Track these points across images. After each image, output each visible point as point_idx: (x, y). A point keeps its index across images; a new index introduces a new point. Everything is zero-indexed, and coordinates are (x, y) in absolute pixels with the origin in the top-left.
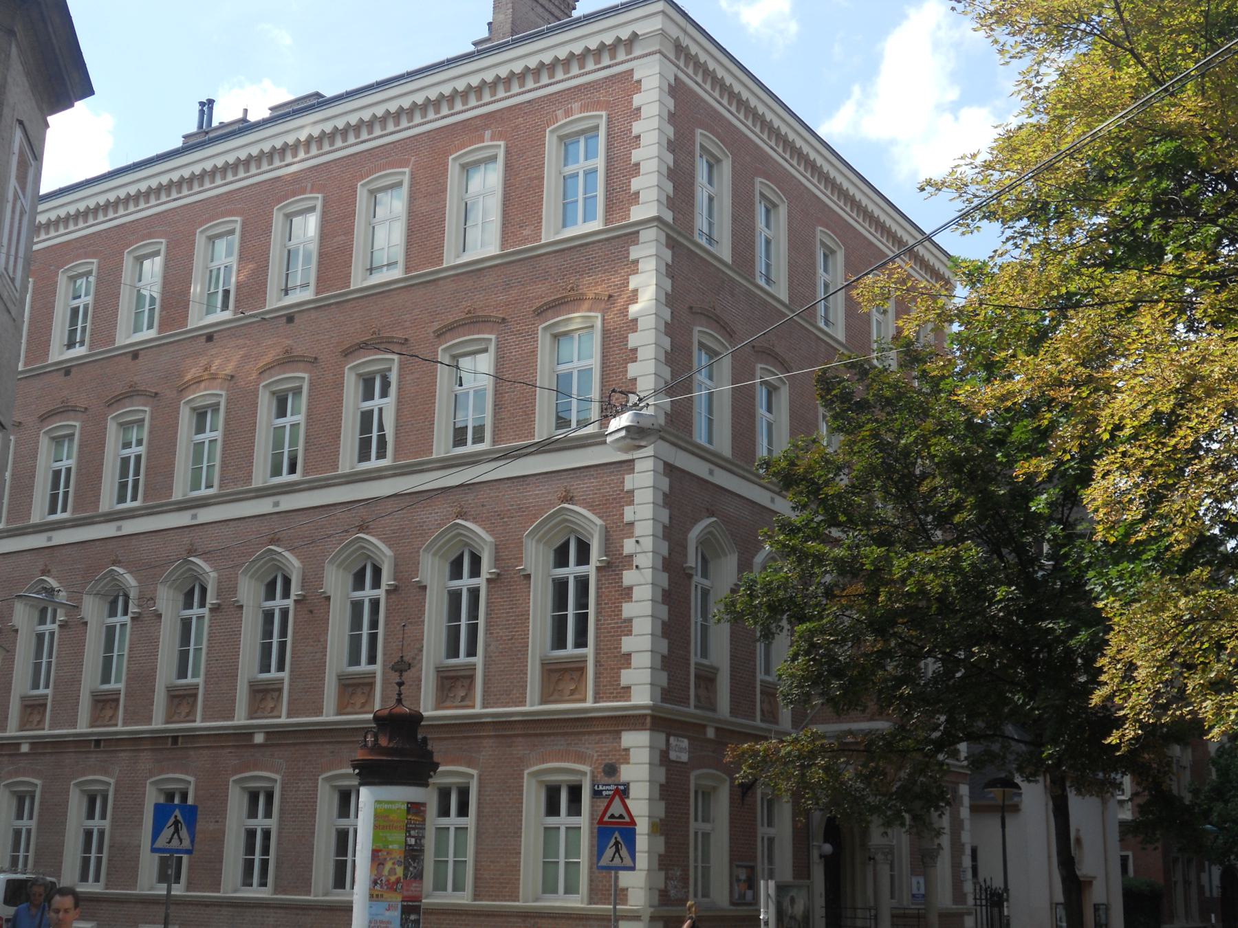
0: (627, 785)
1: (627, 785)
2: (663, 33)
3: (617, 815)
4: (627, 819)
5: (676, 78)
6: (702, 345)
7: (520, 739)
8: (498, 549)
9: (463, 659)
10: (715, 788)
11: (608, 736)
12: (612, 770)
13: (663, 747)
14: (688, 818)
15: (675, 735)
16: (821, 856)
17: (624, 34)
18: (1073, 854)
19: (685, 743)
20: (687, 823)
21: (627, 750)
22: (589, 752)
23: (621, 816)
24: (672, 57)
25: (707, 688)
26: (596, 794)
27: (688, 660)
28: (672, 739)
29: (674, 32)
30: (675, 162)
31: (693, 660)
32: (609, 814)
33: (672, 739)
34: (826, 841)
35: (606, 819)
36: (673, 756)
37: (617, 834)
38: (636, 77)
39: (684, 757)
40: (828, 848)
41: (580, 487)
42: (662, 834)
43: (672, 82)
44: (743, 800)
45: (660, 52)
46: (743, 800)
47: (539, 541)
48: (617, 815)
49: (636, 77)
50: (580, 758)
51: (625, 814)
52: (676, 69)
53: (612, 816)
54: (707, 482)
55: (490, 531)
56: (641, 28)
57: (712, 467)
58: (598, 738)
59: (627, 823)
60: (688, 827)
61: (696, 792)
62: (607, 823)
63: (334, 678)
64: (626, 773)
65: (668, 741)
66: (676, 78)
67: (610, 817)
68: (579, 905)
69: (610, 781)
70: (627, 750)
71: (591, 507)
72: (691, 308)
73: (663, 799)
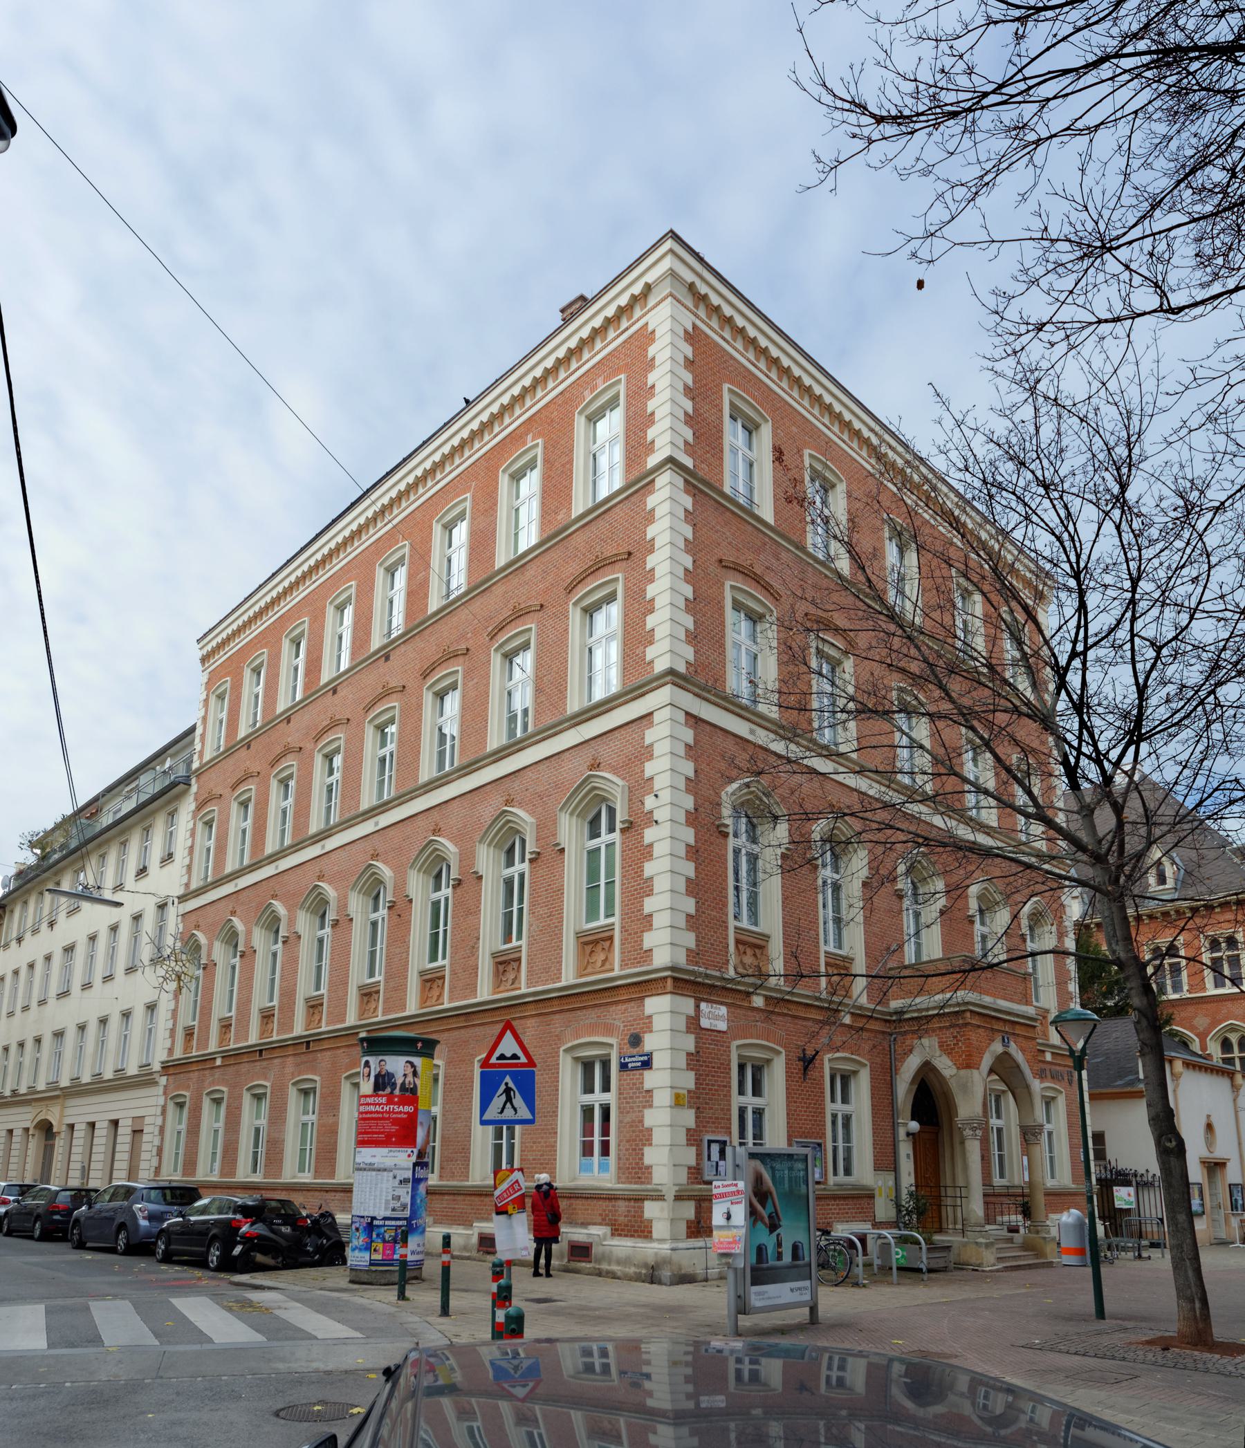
0: (650, 1055)
1: (650, 1055)
2: (672, 273)
3: (508, 1055)
4: (523, 1060)
5: (695, 327)
6: (737, 606)
7: (557, 1016)
8: (540, 827)
9: (514, 943)
10: (769, 1061)
11: (632, 1004)
12: (636, 1040)
13: (692, 1012)
14: (729, 1091)
15: (707, 1001)
16: (908, 1134)
17: (637, 289)
18: (1172, 1105)
19: (723, 1010)
20: (728, 1096)
21: (650, 1017)
22: (617, 1023)
23: (515, 1057)
24: (691, 305)
25: (755, 955)
26: (623, 1066)
27: (725, 922)
28: (703, 1005)
29: (689, 277)
30: (695, 409)
31: (732, 923)
32: (497, 1054)
33: (703, 1005)
34: (913, 1119)
35: (493, 1060)
36: (705, 1023)
37: (508, 1079)
38: (650, 328)
39: (722, 1026)
40: (914, 1126)
41: (605, 751)
42: (690, 1107)
43: (690, 330)
44: (805, 1074)
45: (671, 295)
46: (805, 1074)
47: (572, 814)
48: (508, 1055)
49: (650, 328)
50: (609, 1030)
51: (520, 1053)
52: (693, 318)
53: (502, 1057)
54: (748, 741)
55: (532, 813)
56: (650, 278)
57: (754, 727)
58: (624, 1007)
59: (523, 1065)
60: (729, 1101)
61: (742, 1067)
62: (494, 1065)
63: (415, 974)
64: (650, 1042)
65: (697, 1007)
66: (695, 327)
67: (498, 1059)
68: (609, 1185)
69: (634, 1051)
70: (650, 1017)
71: (615, 770)
72: (721, 561)
73: (692, 1069)
